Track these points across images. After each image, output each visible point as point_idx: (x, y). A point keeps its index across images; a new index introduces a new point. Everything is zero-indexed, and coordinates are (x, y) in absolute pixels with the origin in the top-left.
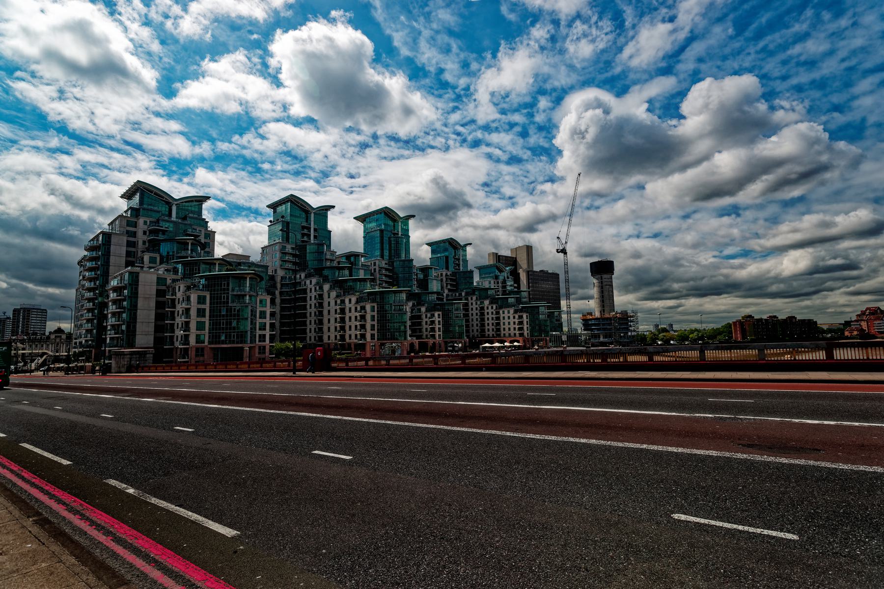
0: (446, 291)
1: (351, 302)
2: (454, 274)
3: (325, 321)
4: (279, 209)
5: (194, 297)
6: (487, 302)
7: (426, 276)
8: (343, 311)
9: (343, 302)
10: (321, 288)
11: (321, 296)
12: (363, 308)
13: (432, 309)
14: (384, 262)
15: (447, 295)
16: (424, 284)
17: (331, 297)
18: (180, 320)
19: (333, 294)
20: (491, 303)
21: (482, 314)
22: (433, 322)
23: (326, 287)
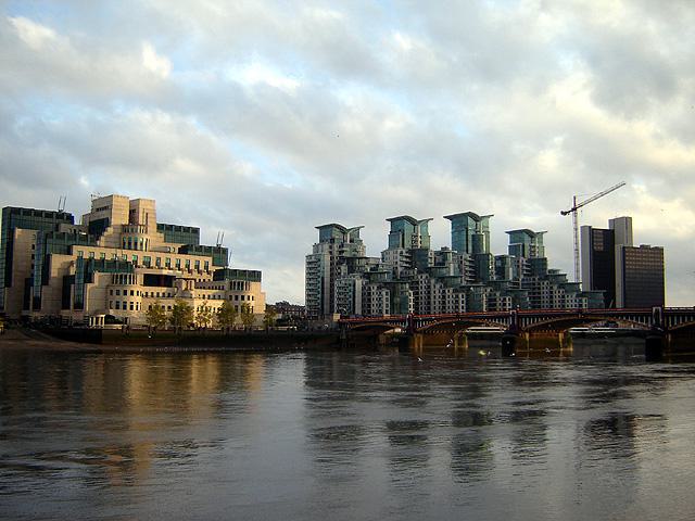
0: (522, 276)
1: (450, 292)
2: (529, 261)
3: (432, 303)
4: (396, 223)
5: (384, 293)
6: (555, 288)
7: (504, 263)
8: (444, 297)
9: (444, 291)
10: (429, 282)
11: (429, 287)
12: (457, 296)
13: (507, 292)
14: (468, 256)
15: (523, 280)
16: (501, 271)
17: (436, 288)
18: (374, 302)
19: (438, 286)
20: (559, 287)
21: (551, 297)
22: (505, 305)
23: (433, 281)
